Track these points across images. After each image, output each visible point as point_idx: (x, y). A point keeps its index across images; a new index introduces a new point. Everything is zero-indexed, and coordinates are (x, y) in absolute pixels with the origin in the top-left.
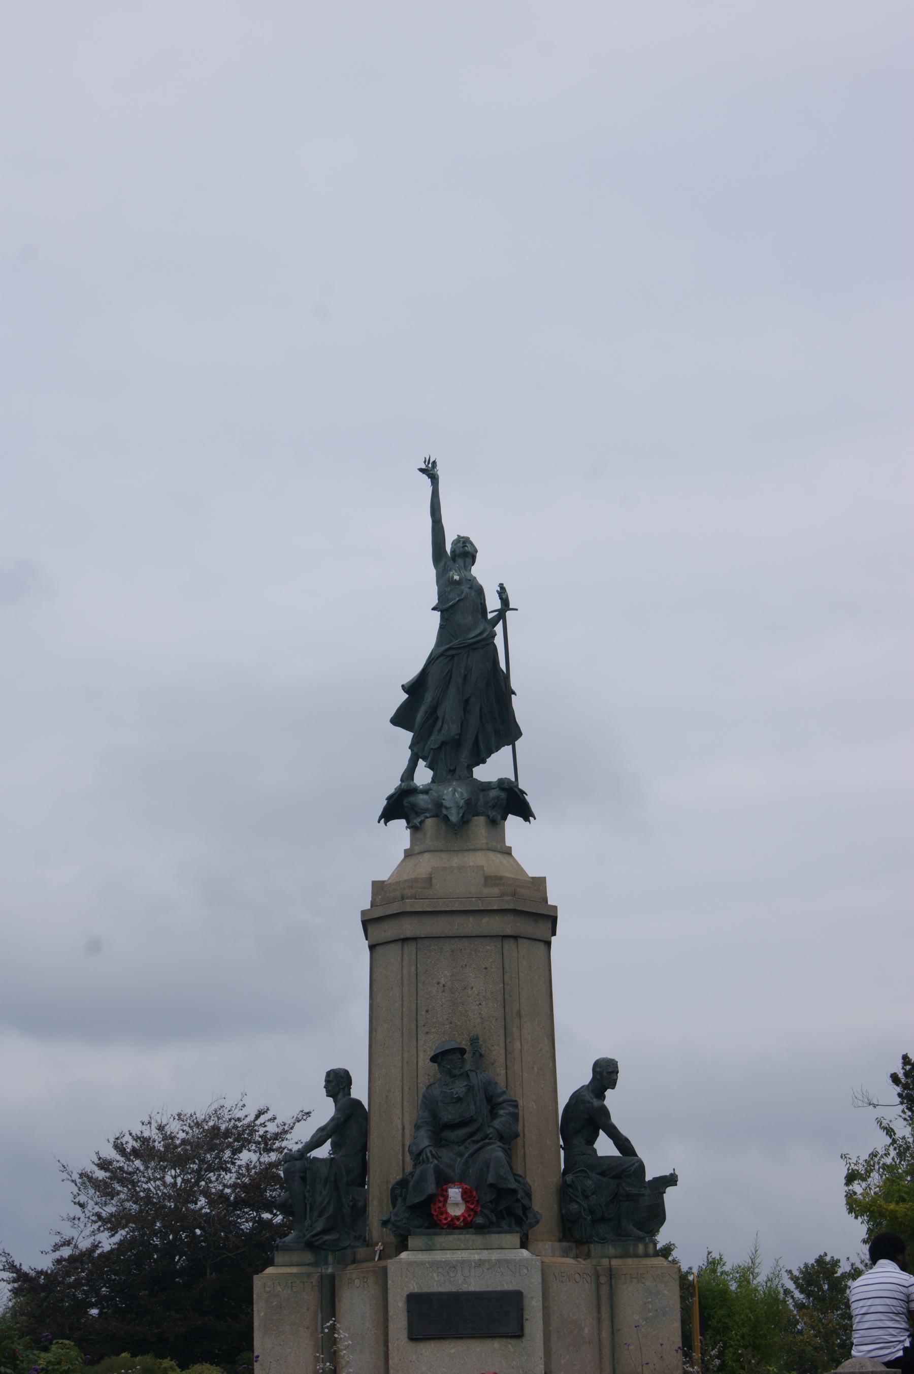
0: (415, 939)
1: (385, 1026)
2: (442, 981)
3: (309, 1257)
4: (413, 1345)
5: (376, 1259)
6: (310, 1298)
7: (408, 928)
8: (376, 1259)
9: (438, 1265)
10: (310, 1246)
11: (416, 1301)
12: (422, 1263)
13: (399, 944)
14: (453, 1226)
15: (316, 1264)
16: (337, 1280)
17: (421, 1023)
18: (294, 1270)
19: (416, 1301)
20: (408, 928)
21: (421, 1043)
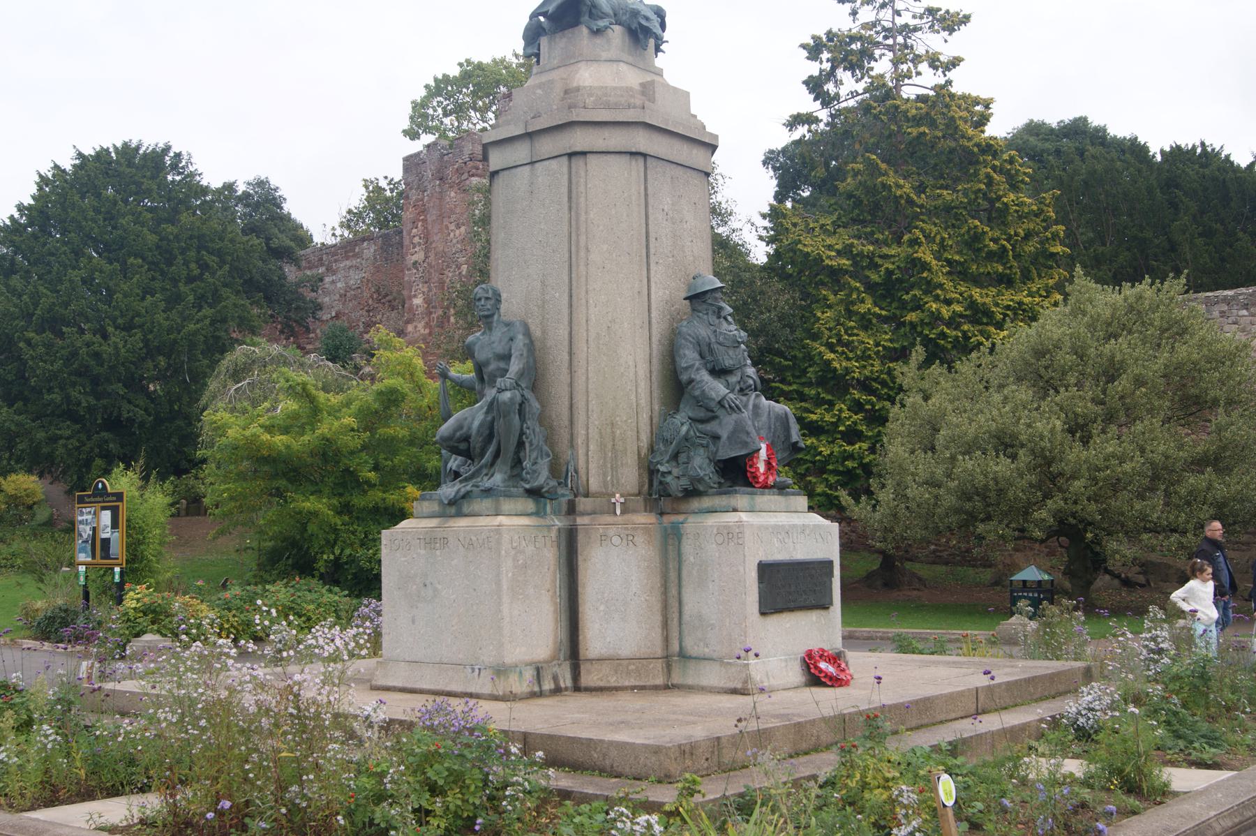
0: (644, 155)
1: (605, 247)
2: (666, 208)
3: (530, 505)
4: (762, 619)
5: (618, 512)
6: (550, 556)
7: (642, 141)
8: (618, 512)
9: (777, 530)
10: (534, 493)
11: (767, 571)
12: (766, 528)
13: (628, 157)
14: (765, 486)
15: (537, 514)
16: (581, 537)
17: (652, 251)
18: (524, 521)
19: (767, 571)
20: (642, 141)
21: (652, 273)
